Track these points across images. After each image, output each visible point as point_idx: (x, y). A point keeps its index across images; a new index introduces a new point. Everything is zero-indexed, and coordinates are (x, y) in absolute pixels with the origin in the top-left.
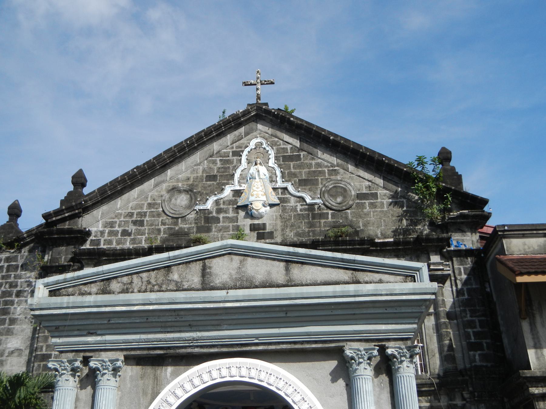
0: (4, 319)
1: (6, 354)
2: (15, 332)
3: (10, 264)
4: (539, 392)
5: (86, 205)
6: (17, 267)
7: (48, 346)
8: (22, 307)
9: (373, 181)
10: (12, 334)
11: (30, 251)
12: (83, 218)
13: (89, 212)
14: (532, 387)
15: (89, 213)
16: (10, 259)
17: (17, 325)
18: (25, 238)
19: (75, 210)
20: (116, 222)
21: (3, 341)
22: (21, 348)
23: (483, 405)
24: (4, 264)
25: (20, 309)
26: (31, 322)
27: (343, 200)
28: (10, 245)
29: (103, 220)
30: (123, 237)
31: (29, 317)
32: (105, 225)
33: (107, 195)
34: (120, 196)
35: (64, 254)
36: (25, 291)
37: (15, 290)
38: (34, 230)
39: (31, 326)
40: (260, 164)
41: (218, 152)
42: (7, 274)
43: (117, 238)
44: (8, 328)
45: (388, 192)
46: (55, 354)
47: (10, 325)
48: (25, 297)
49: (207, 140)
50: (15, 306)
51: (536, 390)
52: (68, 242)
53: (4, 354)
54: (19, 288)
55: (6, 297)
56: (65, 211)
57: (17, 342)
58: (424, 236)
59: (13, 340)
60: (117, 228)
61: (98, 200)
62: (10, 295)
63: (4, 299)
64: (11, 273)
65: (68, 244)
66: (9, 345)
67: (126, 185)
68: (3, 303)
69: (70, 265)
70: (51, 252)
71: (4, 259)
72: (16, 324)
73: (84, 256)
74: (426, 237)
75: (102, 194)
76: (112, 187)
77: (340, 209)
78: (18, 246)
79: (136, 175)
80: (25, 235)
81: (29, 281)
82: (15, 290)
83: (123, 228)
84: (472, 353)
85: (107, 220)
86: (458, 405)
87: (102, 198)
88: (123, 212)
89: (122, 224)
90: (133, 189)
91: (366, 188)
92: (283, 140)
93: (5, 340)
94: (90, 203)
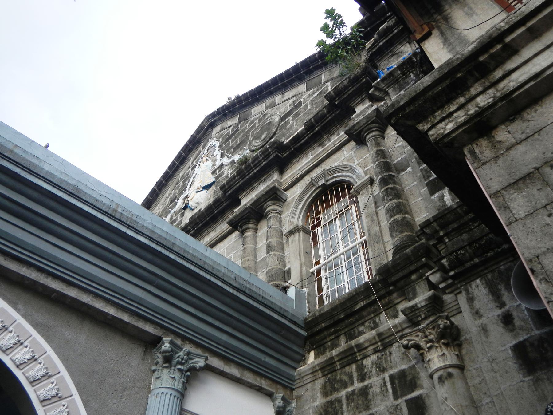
4: (456, 123)
9: (297, 93)
14: (433, 126)
23: (478, 281)
27: (267, 134)
40: (207, 160)
41: (183, 176)
45: (311, 91)
49: (173, 172)
51: (447, 125)
58: (332, 92)
74: (334, 92)
77: (263, 144)
84: (436, 195)
86: (419, 306)
91: (290, 105)
92: (227, 128)
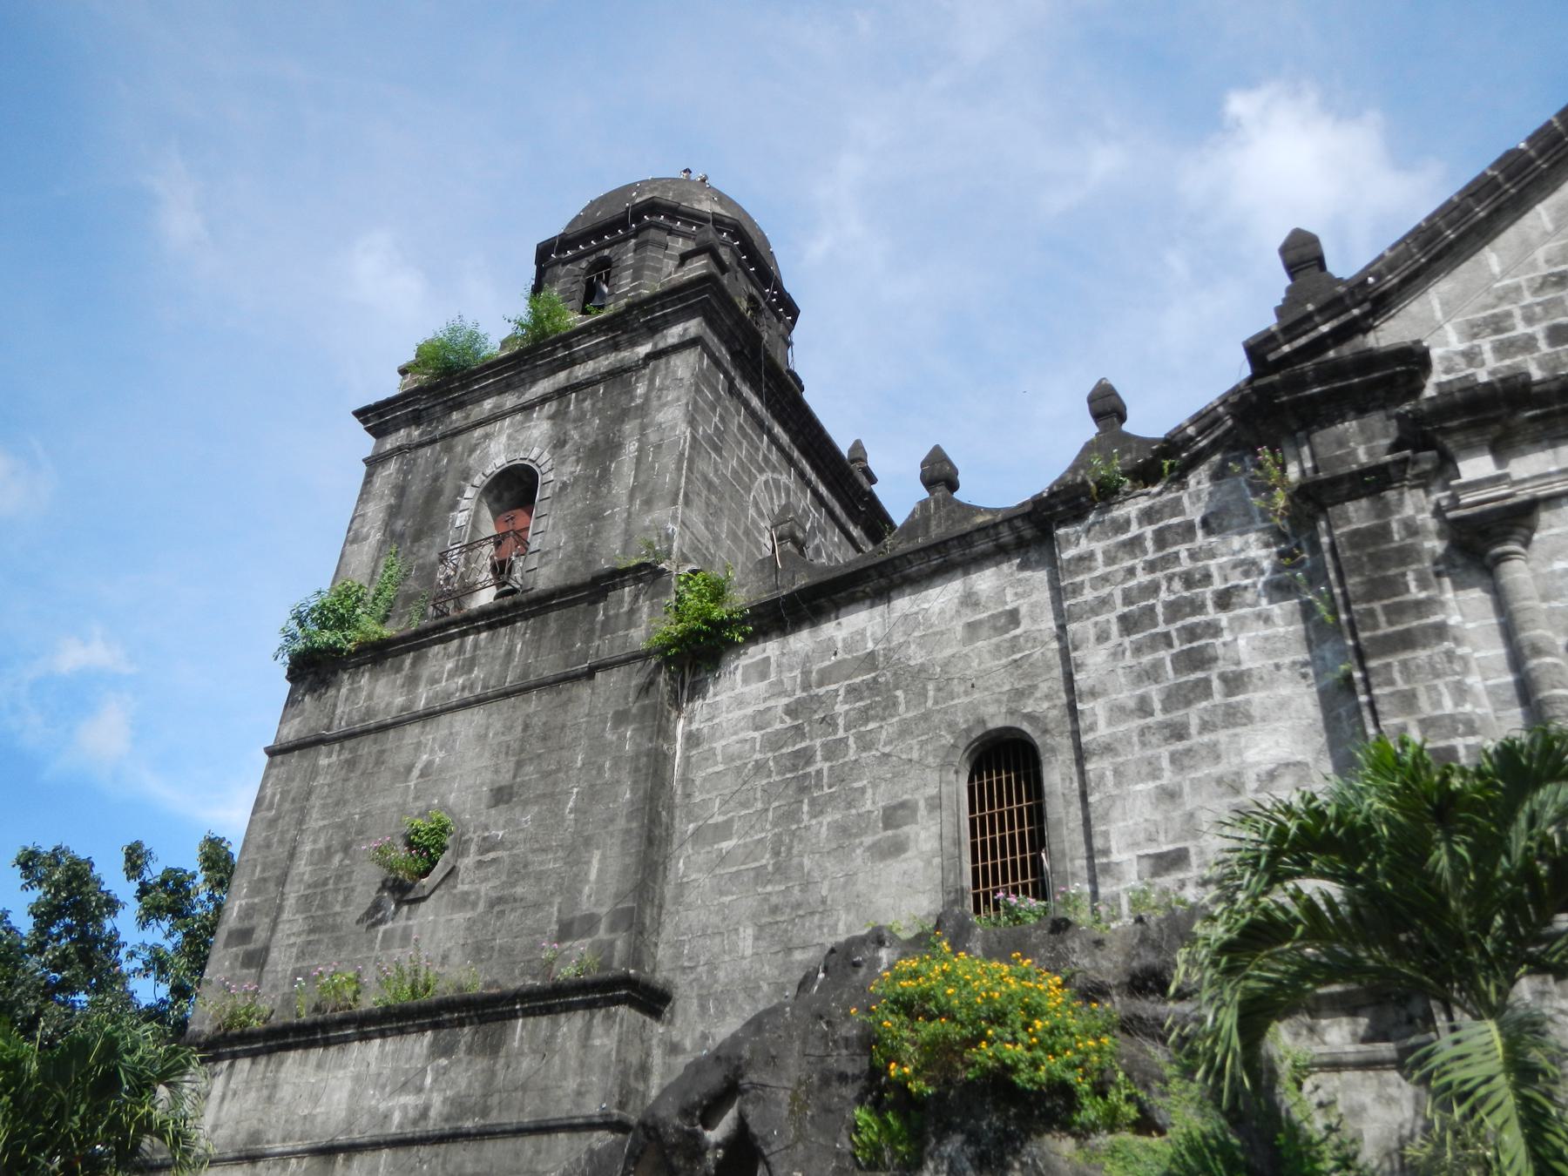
0: (1197, 683)
1: (1251, 784)
2: (1256, 711)
3: (1161, 524)
5: (1383, 288)
6: (1188, 530)
7: (1426, 724)
8: (1253, 634)
10: (1249, 719)
11: (1218, 475)
12: (1380, 334)
13: (1393, 311)
15: (1392, 317)
16: (1158, 512)
17: (1254, 691)
18: (1191, 439)
19: (1348, 310)
20: (1509, 315)
21: (1222, 747)
22: (1299, 758)
24: (1143, 530)
25: (1248, 643)
26: (1304, 676)
28: (1146, 474)
29: (1454, 321)
30: (1559, 348)
31: (1287, 660)
32: (1473, 331)
33: (1446, 242)
34: (1487, 243)
35: (1359, 439)
36: (1246, 588)
37: (1208, 593)
38: (1215, 408)
39: (1309, 686)
42: (1160, 554)
43: (1536, 355)
44: (1229, 706)
46: (1467, 747)
47: (1229, 694)
48: (1250, 606)
50: (1227, 637)
52: (1358, 403)
53: (1243, 784)
54: (1218, 584)
55: (1183, 618)
56: (1317, 319)
57: (1277, 743)
59: (1258, 738)
60: (1521, 329)
61: (1416, 266)
62: (1199, 608)
63: (1179, 624)
64: (1175, 549)
65: (1361, 411)
66: (1251, 755)
67: (1503, 198)
68: (1179, 637)
69: (1405, 460)
70: (1306, 450)
71: (1137, 517)
72: (1251, 688)
73: (1451, 419)
75: (1429, 242)
76: (1455, 214)
78: (1171, 467)
79: (1531, 161)
80: (1191, 431)
81: (1242, 563)
82: (1208, 593)
83: (1545, 324)
85: (1470, 317)
87: (1429, 256)
88: (1522, 280)
89: (1534, 314)
90: (1525, 212)
93: (1230, 743)
94: (1392, 280)
